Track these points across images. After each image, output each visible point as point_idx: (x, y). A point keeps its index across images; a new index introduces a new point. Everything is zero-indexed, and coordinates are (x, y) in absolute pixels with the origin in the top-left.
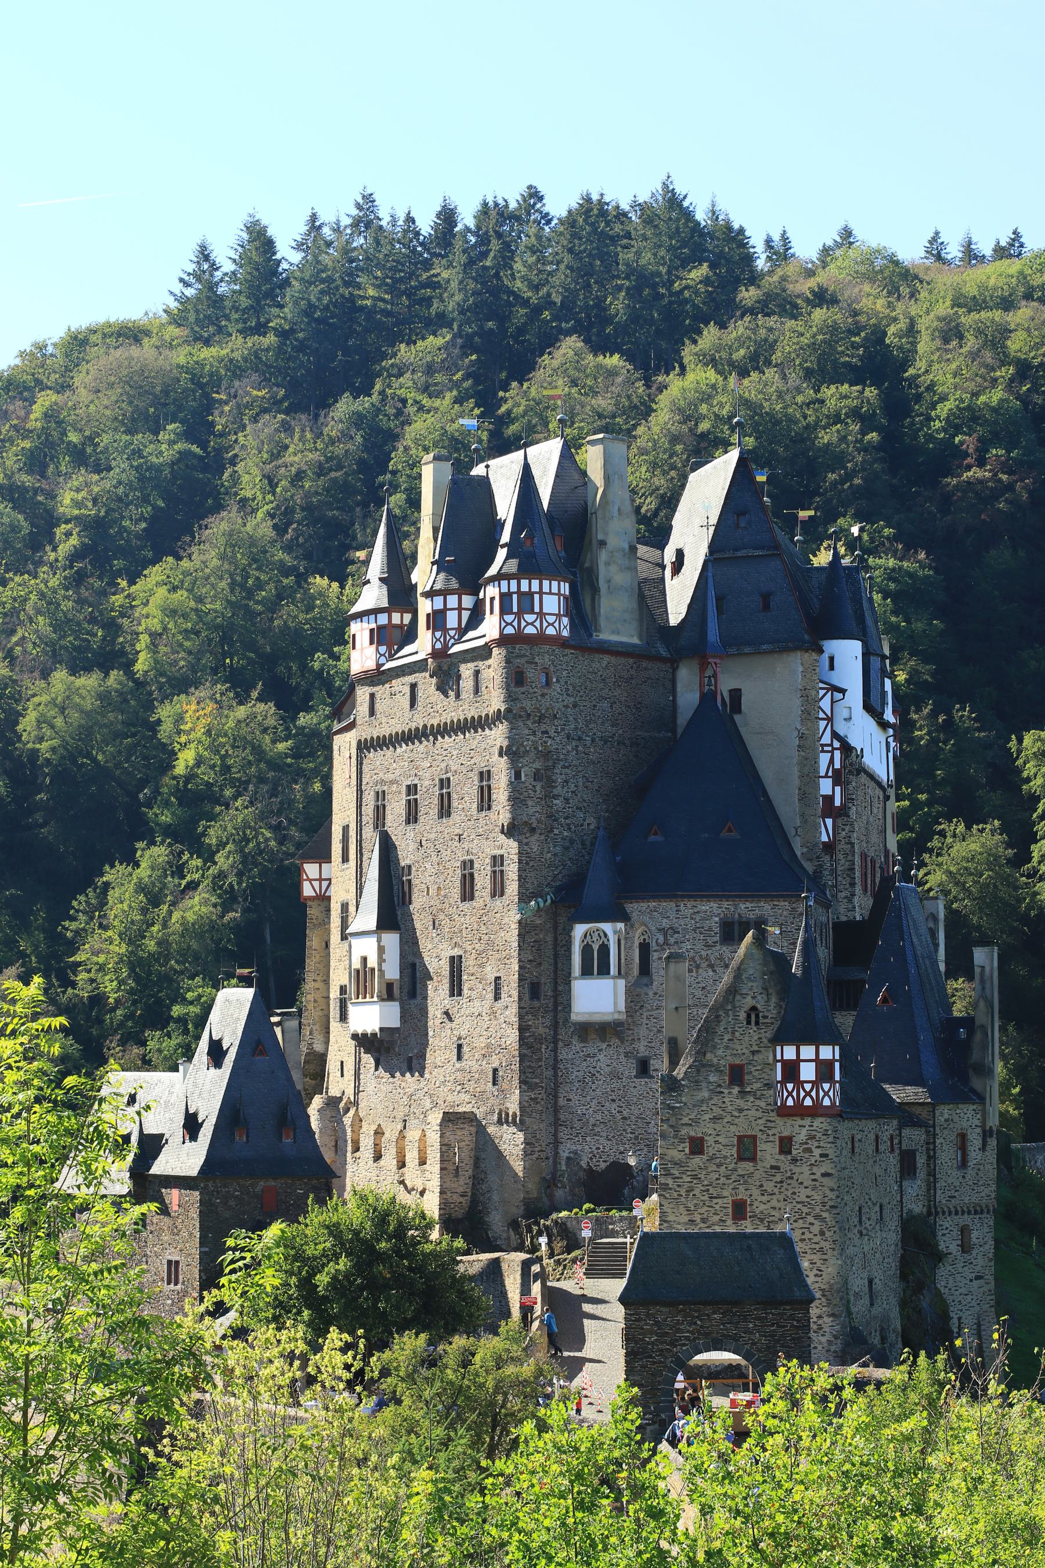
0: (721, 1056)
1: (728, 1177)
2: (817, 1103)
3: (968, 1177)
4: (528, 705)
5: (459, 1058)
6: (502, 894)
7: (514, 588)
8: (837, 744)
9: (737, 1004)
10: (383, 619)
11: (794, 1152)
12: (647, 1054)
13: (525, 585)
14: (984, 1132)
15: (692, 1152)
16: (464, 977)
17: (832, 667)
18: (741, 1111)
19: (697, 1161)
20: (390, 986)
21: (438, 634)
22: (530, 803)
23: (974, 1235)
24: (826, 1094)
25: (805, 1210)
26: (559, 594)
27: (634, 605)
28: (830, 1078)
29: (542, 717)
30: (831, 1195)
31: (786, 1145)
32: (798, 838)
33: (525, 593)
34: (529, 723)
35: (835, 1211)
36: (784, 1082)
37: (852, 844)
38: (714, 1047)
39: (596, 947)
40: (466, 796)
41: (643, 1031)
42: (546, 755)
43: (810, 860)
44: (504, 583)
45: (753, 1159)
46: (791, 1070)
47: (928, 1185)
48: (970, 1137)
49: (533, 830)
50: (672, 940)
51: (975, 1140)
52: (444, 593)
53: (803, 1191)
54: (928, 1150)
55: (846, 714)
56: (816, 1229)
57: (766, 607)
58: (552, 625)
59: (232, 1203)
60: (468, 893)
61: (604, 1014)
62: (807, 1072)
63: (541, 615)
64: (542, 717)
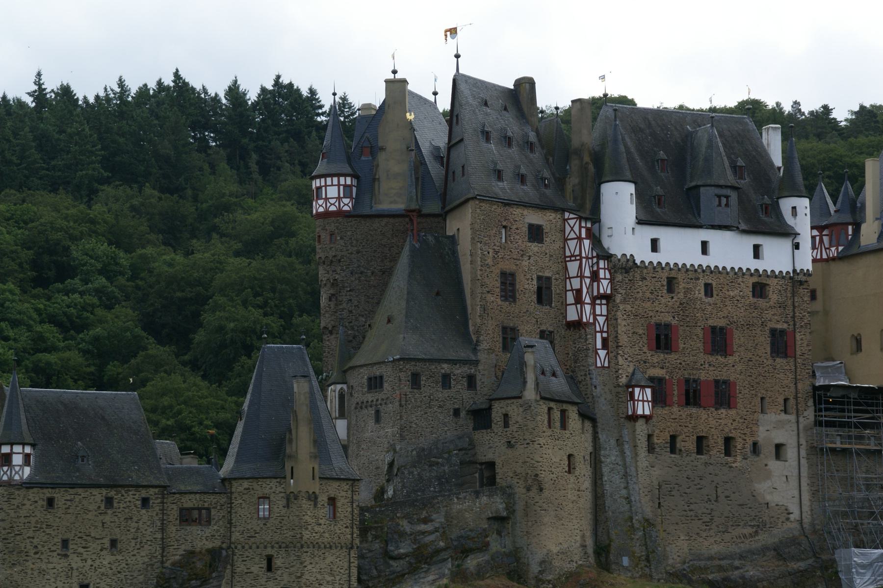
3: (268, 525)
13: (318, 185)
23: (278, 562)
24: (5, 473)
26: (339, 185)
29: (332, 262)
34: (325, 266)
35: (5, 541)
37: (616, 319)
42: (334, 284)
49: (331, 333)
55: (609, 232)
57: (463, 175)
58: (334, 204)
63: (327, 199)
64: (332, 262)
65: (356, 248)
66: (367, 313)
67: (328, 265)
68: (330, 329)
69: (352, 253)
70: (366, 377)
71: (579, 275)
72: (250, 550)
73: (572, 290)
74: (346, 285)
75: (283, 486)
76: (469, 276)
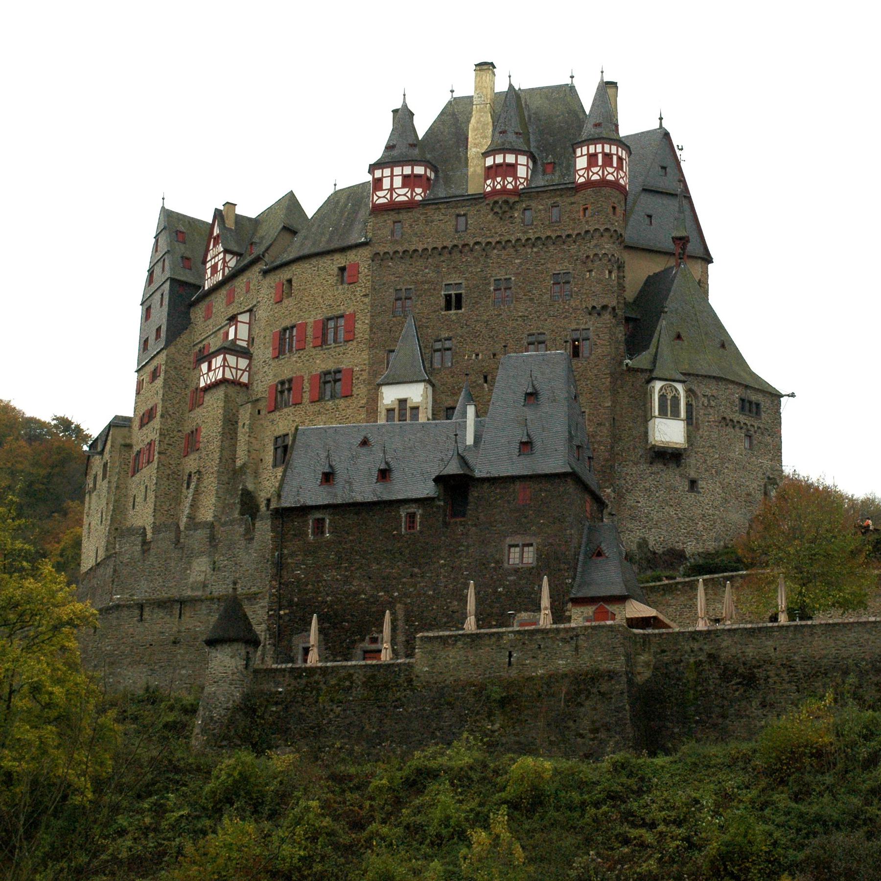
10: (419, 170)
21: (510, 179)
39: (669, 397)
41: (693, 461)
50: (713, 404)
52: (517, 152)
61: (677, 443)
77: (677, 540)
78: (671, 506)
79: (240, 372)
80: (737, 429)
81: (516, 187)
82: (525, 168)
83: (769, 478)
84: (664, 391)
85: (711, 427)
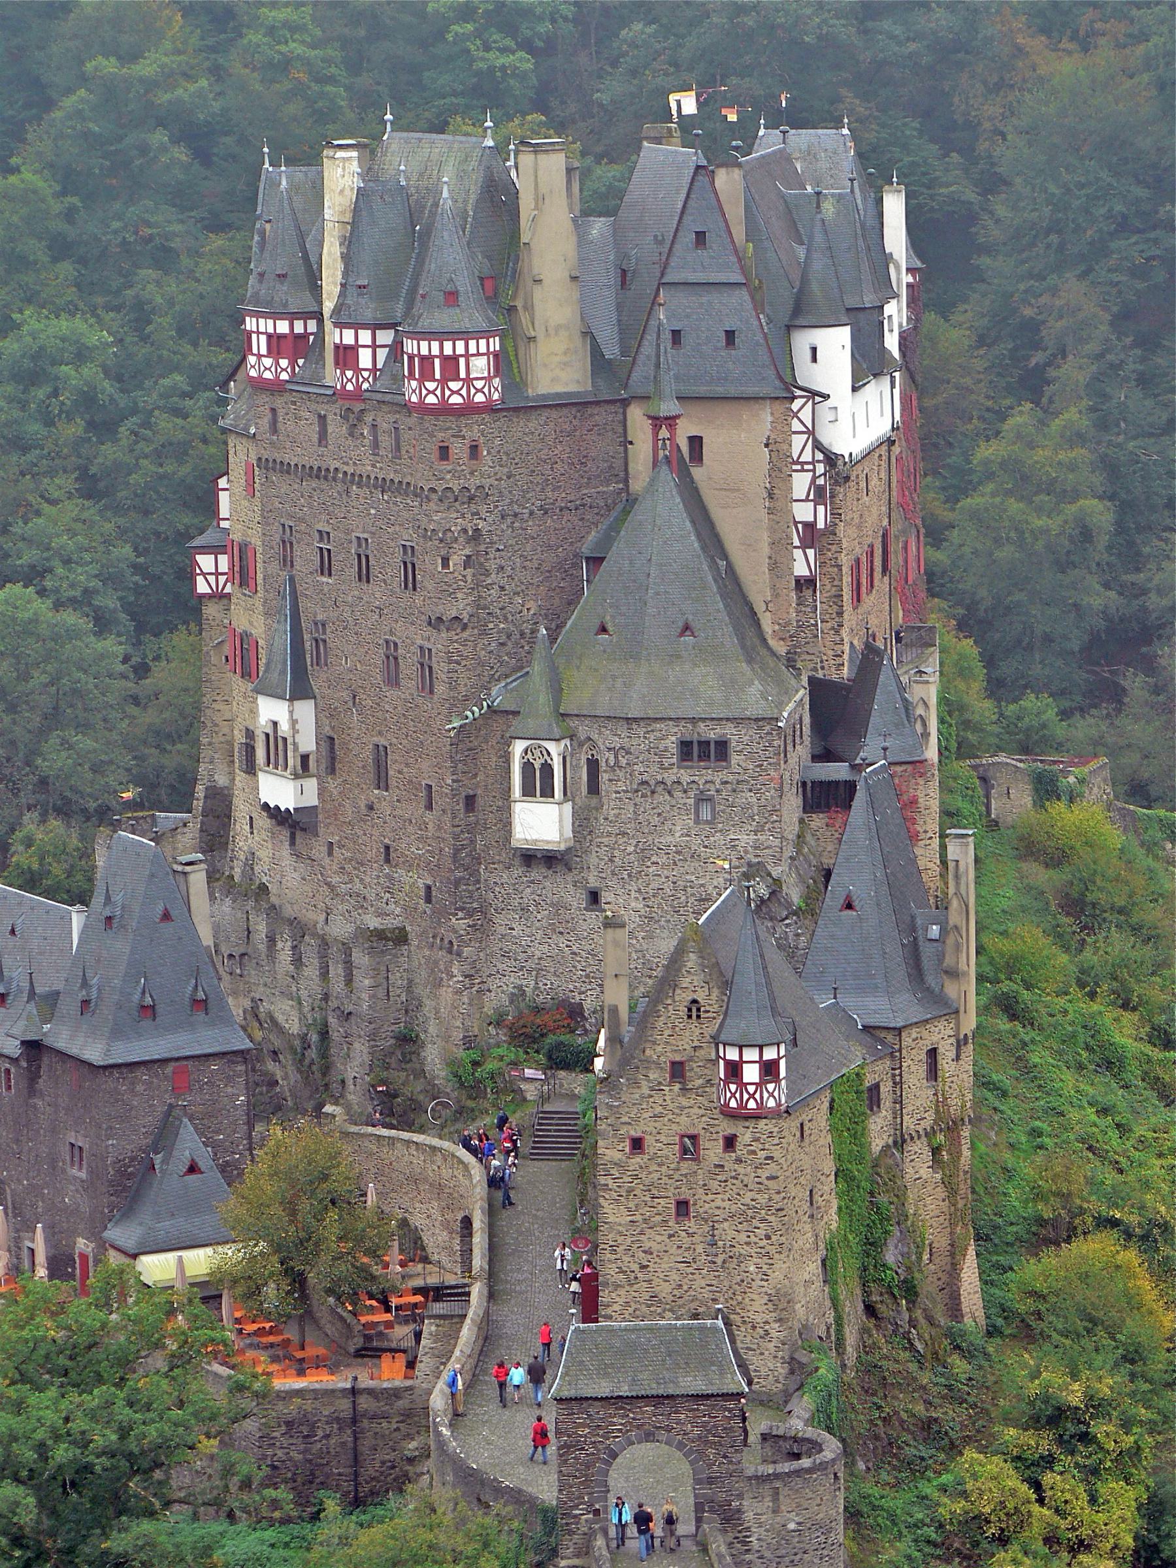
0: (661, 1051)
1: (670, 1177)
2: (760, 1105)
4: (455, 485)
5: (387, 860)
6: (431, 692)
7: (435, 351)
8: (819, 456)
9: (677, 998)
10: (283, 327)
11: (739, 1153)
12: (597, 884)
13: (448, 349)
14: (958, 1041)
15: (631, 1153)
16: (391, 773)
17: (814, 360)
18: (682, 1108)
19: (637, 1160)
20: (305, 758)
21: (349, 374)
22: (459, 595)
25: (750, 1213)
27: (578, 341)
28: (776, 1079)
29: (471, 498)
30: (777, 1197)
31: (730, 1142)
32: (768, 614)
33: (448, 358)
35: (781, 1214)
36: (727, 1082)
37: (840, 567)
38: (654, 1043)
39: (537, 766)
40: (389, 569)
41: (593, 860)
43: (783, 639)
44: (424, 345)
45: (696, 1160)
46: (734, 1070)
47: (894, 1113)
48: (941, 1050)
49: (465, 627)
50: (623, 762)
51: (947, 1052)
52: (357, 327)
53: (750, 1195)
54: (894, 1076)
56: (761, 1232)
59: (140, 1088)
60: (393, 680)
61: (548, 842)
62: (751, 1073)
63: (468, 381)
65: (506, 470)
66: (524, 587)
67: (464, 503)
68: (465, 621)
69: (500, 479)
70: (674, 738)
71: (811, 497)
72: (918, 1142)
73: (796, 523)
74: (495, 538)
75: (952, 1025)
76: (765, 538)
77: (571, 987)
78: (561, 933)
79: (222, 579)
80: (678, 794)
81: (358, 387)
82: (370, 350)
83: (750, 865)
84: (529, 755)
85: (620, 799)
